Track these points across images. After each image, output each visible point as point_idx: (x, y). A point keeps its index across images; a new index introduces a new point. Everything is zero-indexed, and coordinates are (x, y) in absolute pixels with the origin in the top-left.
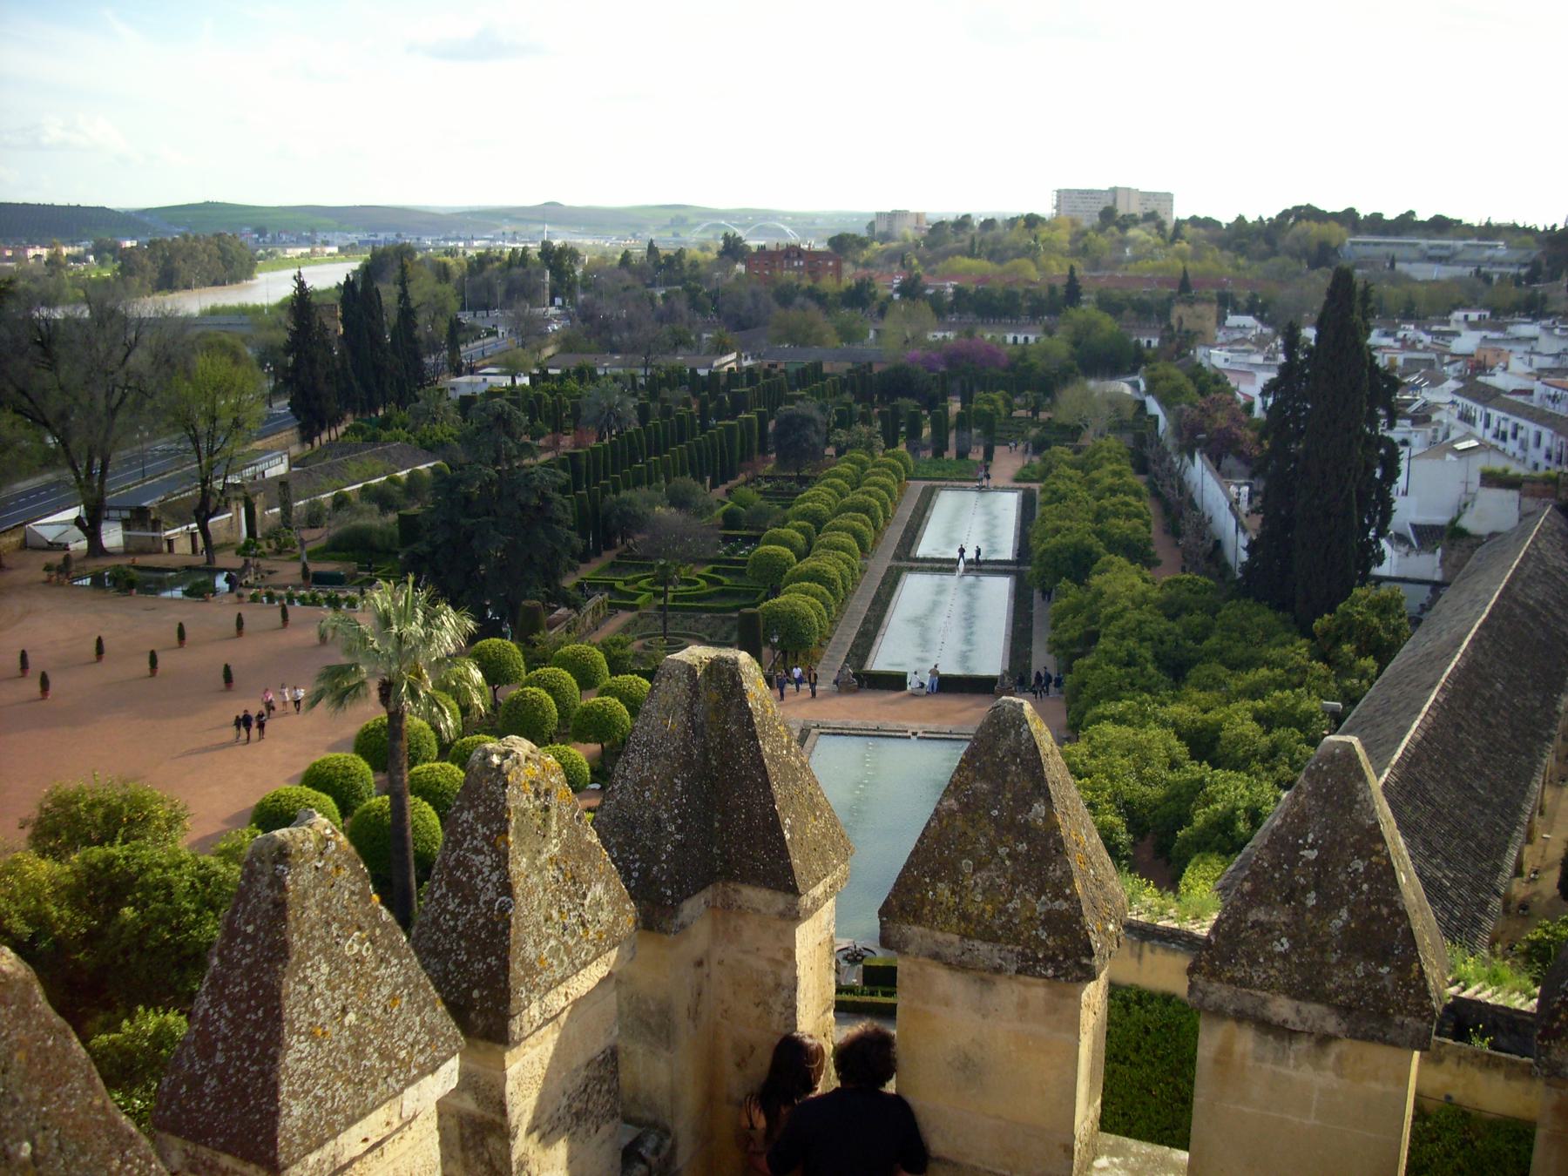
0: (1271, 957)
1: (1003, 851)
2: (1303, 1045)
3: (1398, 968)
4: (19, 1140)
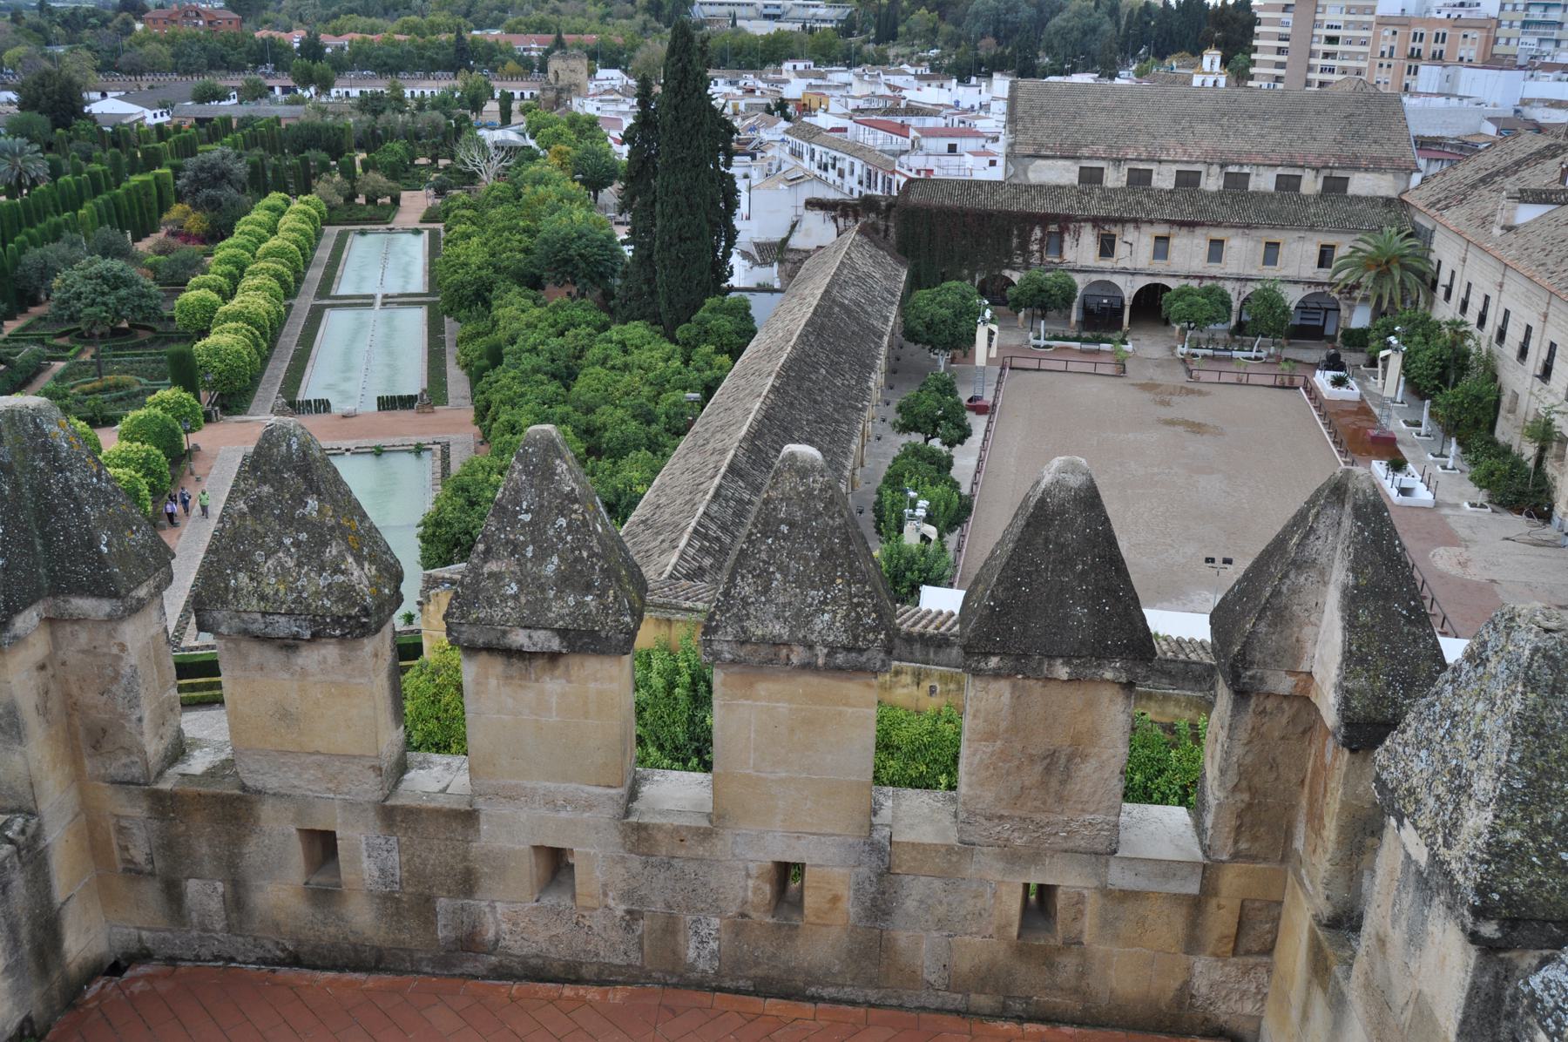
0: (504, 599)
1: (288, 541)
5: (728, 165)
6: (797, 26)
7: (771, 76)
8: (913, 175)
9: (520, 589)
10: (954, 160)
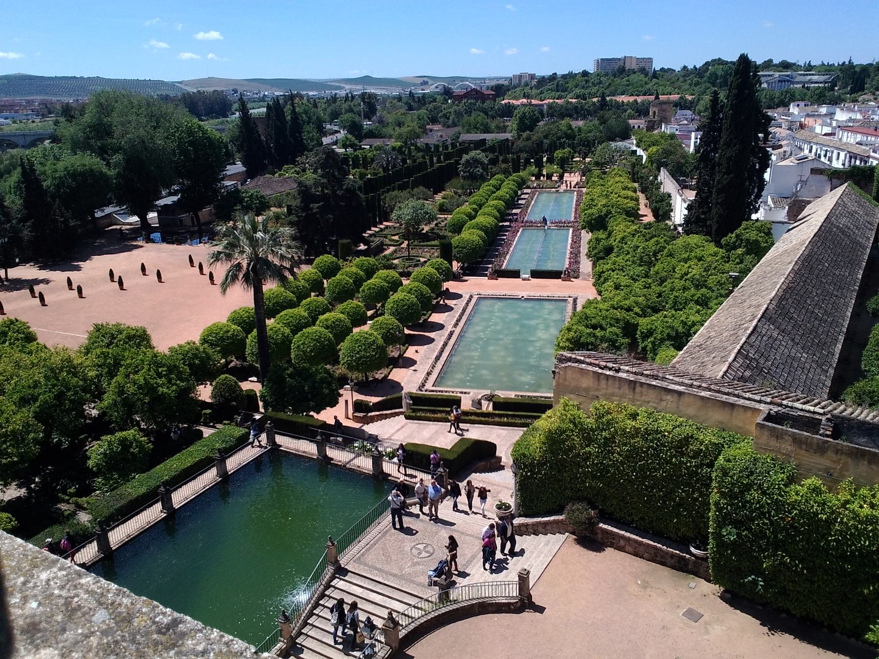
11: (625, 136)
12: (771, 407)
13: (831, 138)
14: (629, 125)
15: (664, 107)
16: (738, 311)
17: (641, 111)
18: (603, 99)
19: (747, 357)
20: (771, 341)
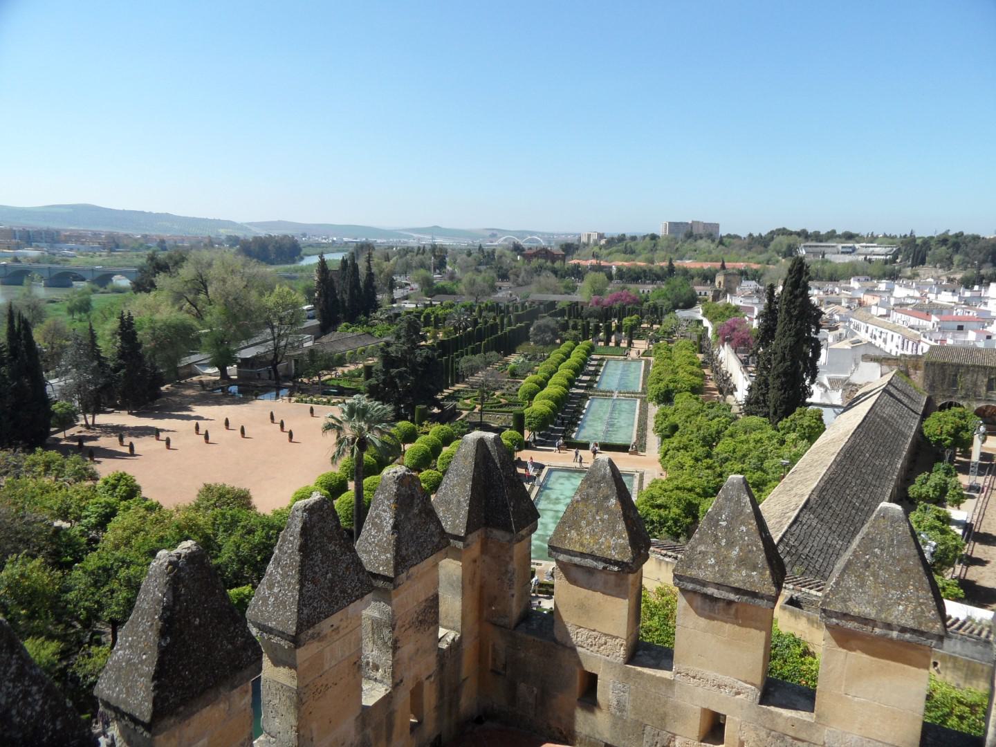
0: (707, 566)
1: (598, 518)
2: (721, 604)
3: (761, 573)
4: (195, 617)
5: (817, 332)
6: (861, 258)
7: (843, 285)
8: (933, 343)
9: (716, 563)
10: (961, 338)
11: (690, 303)
12: (793, 593)
13: (886, 320)
14: (694, 292)
15: (730, 278)
16: (785, 498)
17: (708, 277)
18: (671, 264)
19: (787, 544)
20: (810, 529)
